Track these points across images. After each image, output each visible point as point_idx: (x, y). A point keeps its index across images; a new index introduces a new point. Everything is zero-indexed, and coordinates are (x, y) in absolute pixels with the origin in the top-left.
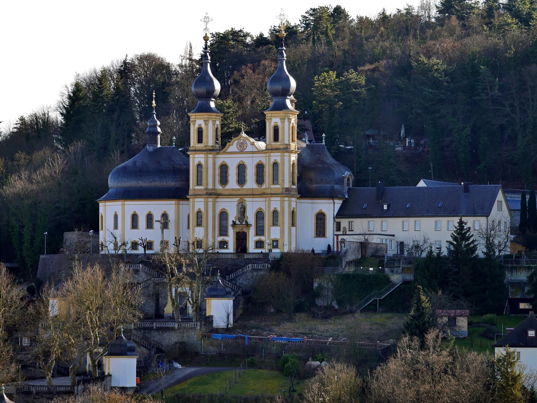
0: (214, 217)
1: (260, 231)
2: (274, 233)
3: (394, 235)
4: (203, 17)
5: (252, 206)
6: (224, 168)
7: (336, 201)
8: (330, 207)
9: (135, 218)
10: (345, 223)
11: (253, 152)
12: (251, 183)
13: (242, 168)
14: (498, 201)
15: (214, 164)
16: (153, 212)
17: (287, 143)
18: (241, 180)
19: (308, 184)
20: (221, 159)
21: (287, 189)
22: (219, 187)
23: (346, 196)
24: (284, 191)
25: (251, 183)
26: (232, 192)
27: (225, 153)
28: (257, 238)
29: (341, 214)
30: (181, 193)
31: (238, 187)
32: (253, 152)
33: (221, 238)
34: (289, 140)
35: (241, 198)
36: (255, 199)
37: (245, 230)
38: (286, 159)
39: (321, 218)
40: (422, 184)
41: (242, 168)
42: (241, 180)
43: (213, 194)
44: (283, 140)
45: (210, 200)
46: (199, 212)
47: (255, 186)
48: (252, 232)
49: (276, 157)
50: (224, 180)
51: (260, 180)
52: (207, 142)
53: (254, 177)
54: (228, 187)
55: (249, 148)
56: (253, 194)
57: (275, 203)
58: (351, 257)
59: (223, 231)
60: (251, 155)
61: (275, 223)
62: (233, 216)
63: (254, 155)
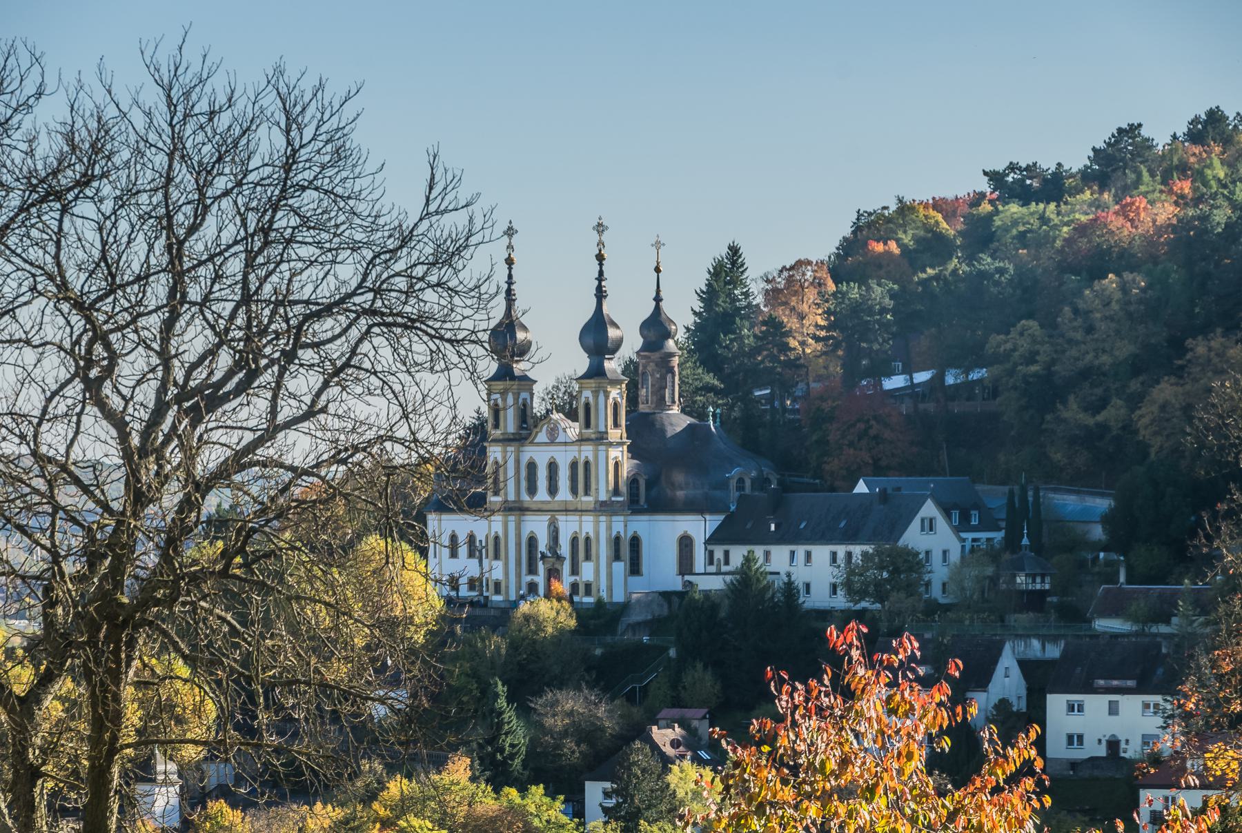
0: (518, 545)
1: (575, 571)
2: (587, 571)
3: (778, 573)
4: (506, 228)
5: (568, 526)
6: (532, 467)
7: (708, 517)
8: (699, 527)
9: (454, 538)
10: (719, 553)
11: (566, 444)
12: (564, 494)
13: (553, 467)
14: (923, 520)
15: (518, 462)
16: (476, 533)
17: (602, 429)
18: (553, 489)
19: (668, 491)
20: (529, 453)
21: (603, 503)
22: (525, 497)
23: (733, 508)
24: (598, 506)
25: (564, 494)
26: (540, 506)
27: (532, 443)
28: (572, 579)
29: (714, 539)
30: (477, 504)
31: (549, 499)
32: (566, 444)
33: (529, 578)
34: (606, 426)
35: (553, 516)
36: (570, 518)
37: (557, 566)
38: (602, 455)
39: (686, 543)
40: (861, 488)
41: (553, 467)
42: (553, 489)
43: (516, 509)
44: (597, 426)
45: (512, 518)
46: (497, 538)
47: (570, 497)
48: (566, 567)
49: (587, 451)
50: (532, 490)
51: (574, 490)
52: (505, 427)
53: (568, 483)
54: (535, 499)
55: (561, 439)
56: (566, 511)
57: (587, 525)
58: (636, 617)
59: (532, 570)
60: (563, 448)
61: (588, 558)
62: (542, 546)
63: (568, 448)
